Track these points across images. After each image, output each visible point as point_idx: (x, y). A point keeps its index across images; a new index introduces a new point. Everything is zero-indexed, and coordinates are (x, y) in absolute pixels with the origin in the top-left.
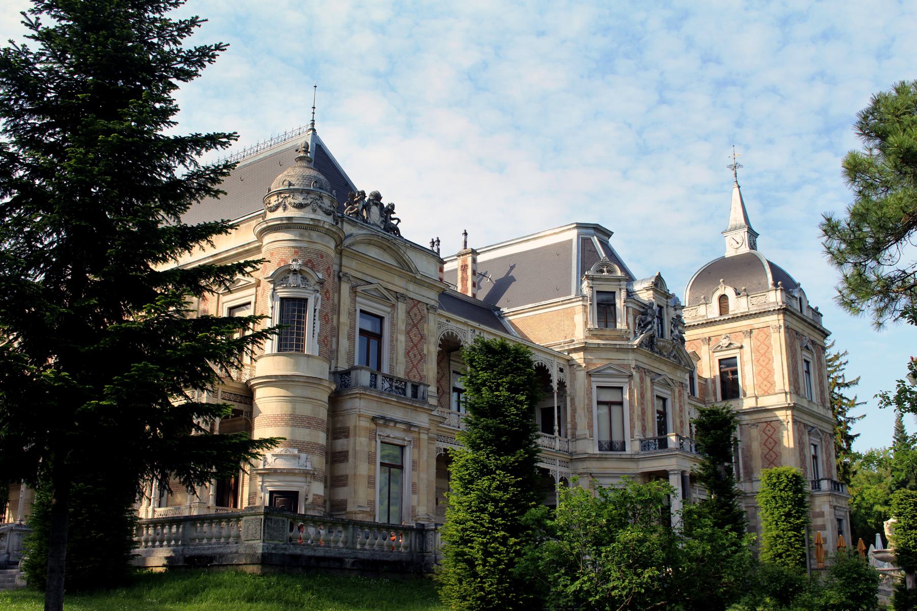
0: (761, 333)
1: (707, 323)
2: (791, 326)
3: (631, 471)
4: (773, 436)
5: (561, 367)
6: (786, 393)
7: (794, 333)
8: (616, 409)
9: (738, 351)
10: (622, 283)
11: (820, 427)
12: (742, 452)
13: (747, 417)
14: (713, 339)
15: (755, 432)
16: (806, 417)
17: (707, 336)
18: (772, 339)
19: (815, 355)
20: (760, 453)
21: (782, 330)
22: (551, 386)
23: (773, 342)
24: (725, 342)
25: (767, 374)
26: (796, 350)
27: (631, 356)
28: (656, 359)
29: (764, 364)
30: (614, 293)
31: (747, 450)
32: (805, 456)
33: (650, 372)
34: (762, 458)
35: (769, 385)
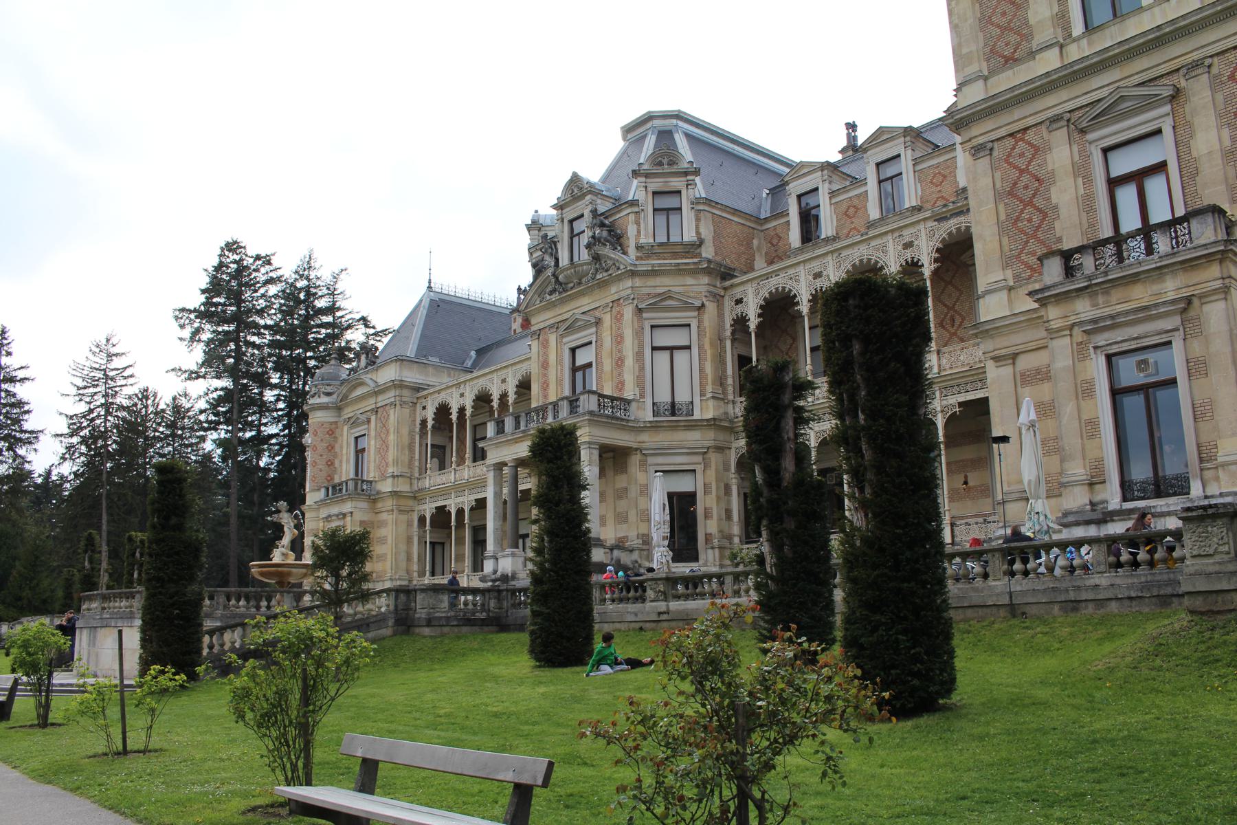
11: (1137, 79)
28: (563, 301)
33: (552, 326)
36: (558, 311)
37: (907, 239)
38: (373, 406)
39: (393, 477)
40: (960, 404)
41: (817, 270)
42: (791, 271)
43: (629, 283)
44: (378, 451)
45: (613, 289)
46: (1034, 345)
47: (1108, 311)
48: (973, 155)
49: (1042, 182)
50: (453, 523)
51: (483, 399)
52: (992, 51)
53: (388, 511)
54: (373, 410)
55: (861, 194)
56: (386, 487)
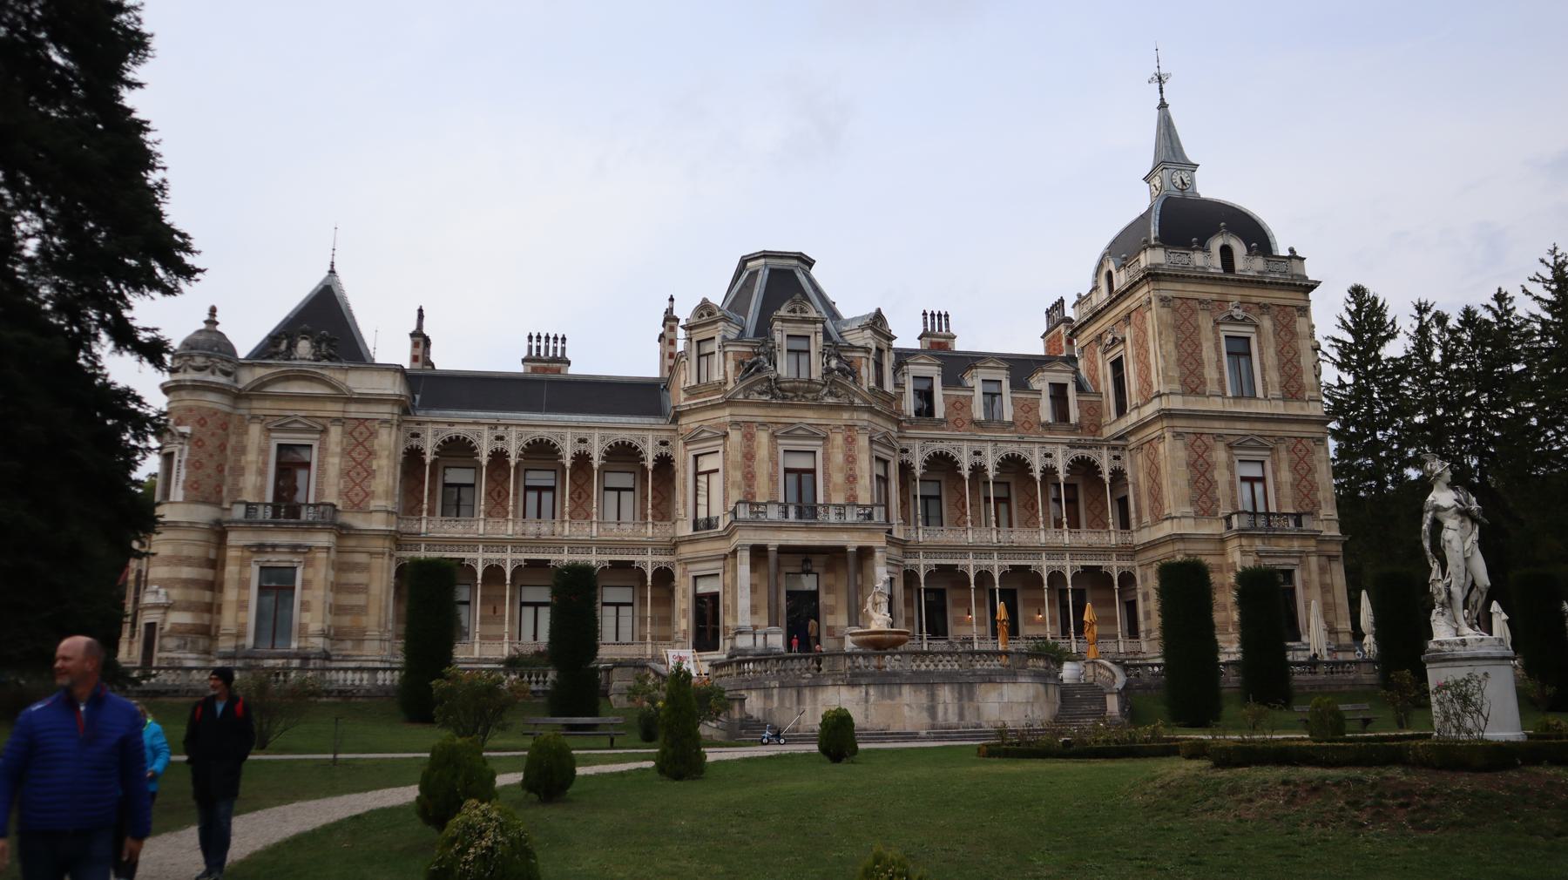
2: (1169, 294)
3: (723, 552)
4: (1156, 462)
5: (664, 439)
8: (713, 477)
9: (1122, 347)
10: (719, 324)
13: (1133, 439)
15: (1140, 458)
16: (1217, 424)
19: (1266, 323)
22: (643, 465)
26: (1197, 328)
27: (727, 411)
28: (781, 406)
29: (1142, 358)
30: (714, 338)
31: (1136, 485)
32: (1212, 484)
33: (763, 424)
36: (770, 412)
37: (1049, 451)
38: (340, 415)
39: (388, 512)
40: (1082, 567)
41: (977, 449)
42: (953, 443)
43: (866, 416)
44: (345, 474)
45: (846, 415)
46: (1207, 552)
47: (1268, 548)
49: (1210, 466)
50: (508, 582)
51: (541, 452)
52: (1184, 381)
53: (371, 554)
54: (336, 420)
55: (967, 396)
56: (378, 523)
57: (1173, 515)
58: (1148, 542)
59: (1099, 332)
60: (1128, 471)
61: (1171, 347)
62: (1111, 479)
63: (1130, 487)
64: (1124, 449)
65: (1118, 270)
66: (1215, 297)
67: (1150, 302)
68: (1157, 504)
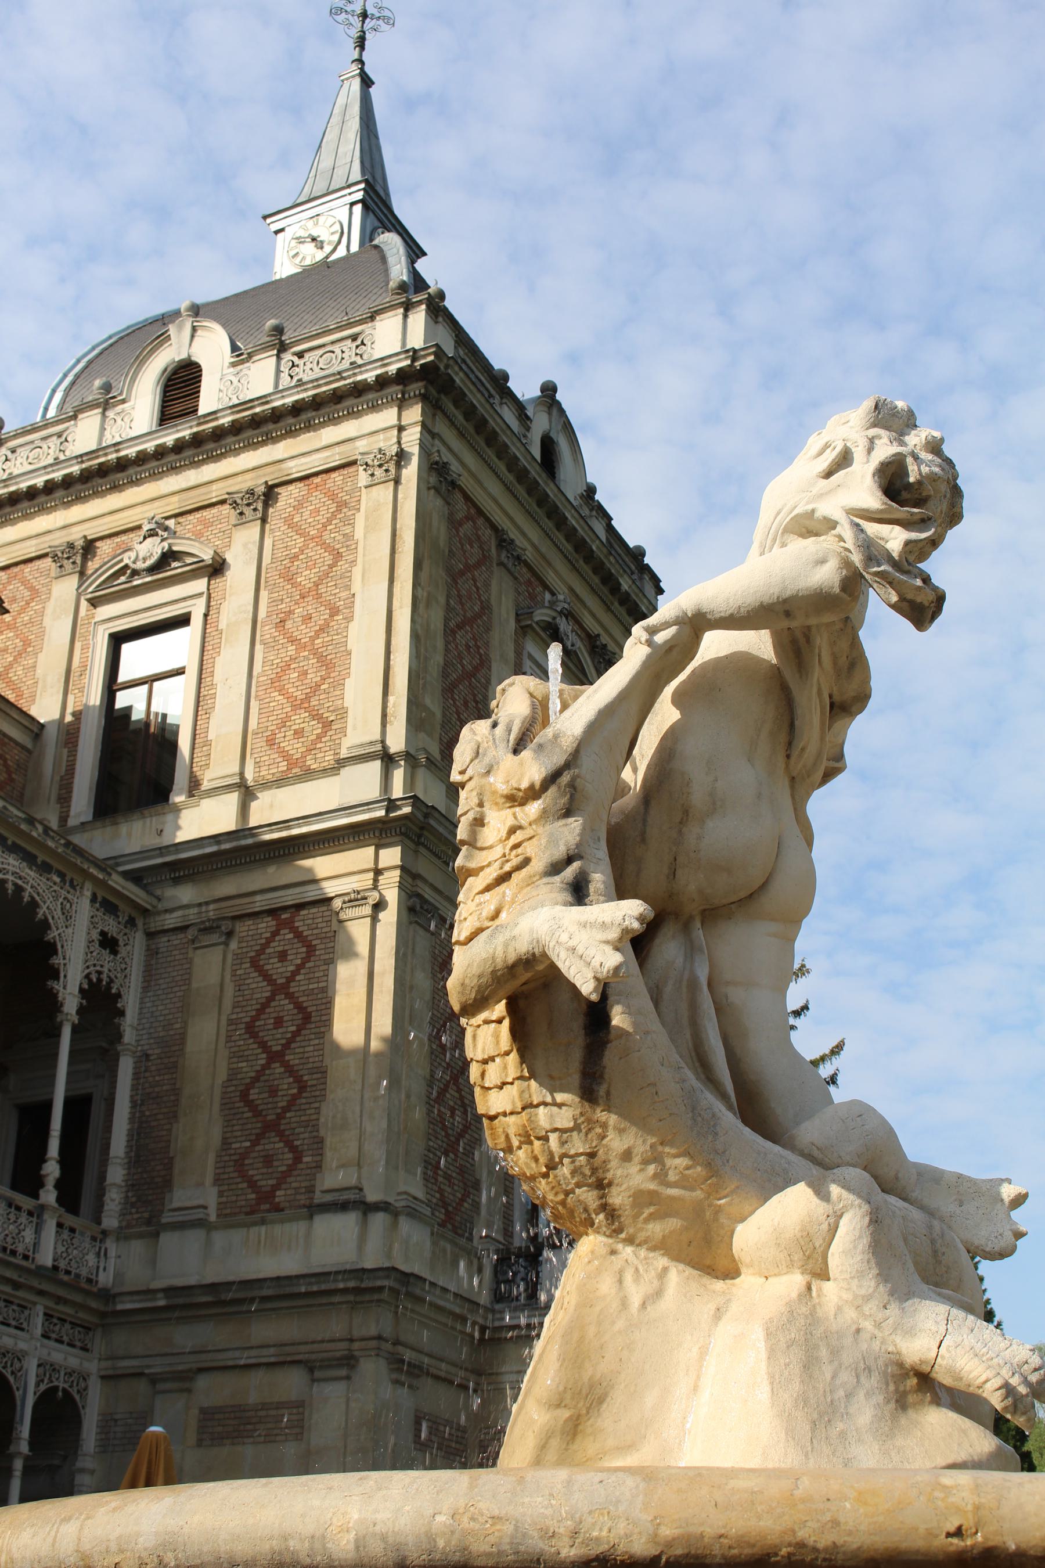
0: (318, 498)
1: (86, 477)
2: (455, 467)
6: (388, 760)
7: (487, 533)
9: (200, 585)
12: (136, 1076)
13: (185, 894)
14: (105, 549)
17: (76, 535)
18: (360, 520)
20: (222, 1075)
21: (411, 473)
23: (359, 533)
24: (151, 549)
25: (313, 677)
26: (486, 608)
34: (226, 1104)
35: (313, 728)
48: (411, 910)
57: (372, 1196)
58: (213, 1287)
59: (92, 530)
60: (131, 1003)
61: (436, 617)
62: (81, 1011)
63: (126, 1068)
64: (131, 922)
65: (240, 356)
66: (529, 555)
67: (401, 457)
68: (274, 1144)
